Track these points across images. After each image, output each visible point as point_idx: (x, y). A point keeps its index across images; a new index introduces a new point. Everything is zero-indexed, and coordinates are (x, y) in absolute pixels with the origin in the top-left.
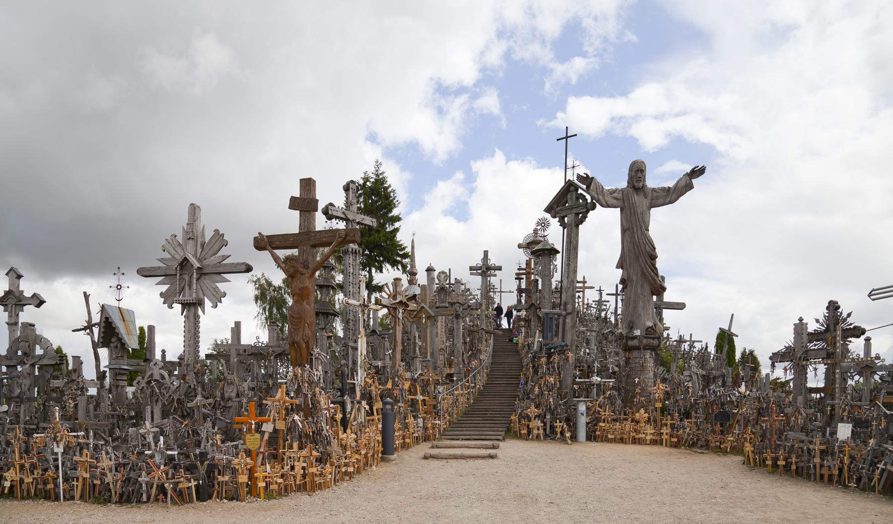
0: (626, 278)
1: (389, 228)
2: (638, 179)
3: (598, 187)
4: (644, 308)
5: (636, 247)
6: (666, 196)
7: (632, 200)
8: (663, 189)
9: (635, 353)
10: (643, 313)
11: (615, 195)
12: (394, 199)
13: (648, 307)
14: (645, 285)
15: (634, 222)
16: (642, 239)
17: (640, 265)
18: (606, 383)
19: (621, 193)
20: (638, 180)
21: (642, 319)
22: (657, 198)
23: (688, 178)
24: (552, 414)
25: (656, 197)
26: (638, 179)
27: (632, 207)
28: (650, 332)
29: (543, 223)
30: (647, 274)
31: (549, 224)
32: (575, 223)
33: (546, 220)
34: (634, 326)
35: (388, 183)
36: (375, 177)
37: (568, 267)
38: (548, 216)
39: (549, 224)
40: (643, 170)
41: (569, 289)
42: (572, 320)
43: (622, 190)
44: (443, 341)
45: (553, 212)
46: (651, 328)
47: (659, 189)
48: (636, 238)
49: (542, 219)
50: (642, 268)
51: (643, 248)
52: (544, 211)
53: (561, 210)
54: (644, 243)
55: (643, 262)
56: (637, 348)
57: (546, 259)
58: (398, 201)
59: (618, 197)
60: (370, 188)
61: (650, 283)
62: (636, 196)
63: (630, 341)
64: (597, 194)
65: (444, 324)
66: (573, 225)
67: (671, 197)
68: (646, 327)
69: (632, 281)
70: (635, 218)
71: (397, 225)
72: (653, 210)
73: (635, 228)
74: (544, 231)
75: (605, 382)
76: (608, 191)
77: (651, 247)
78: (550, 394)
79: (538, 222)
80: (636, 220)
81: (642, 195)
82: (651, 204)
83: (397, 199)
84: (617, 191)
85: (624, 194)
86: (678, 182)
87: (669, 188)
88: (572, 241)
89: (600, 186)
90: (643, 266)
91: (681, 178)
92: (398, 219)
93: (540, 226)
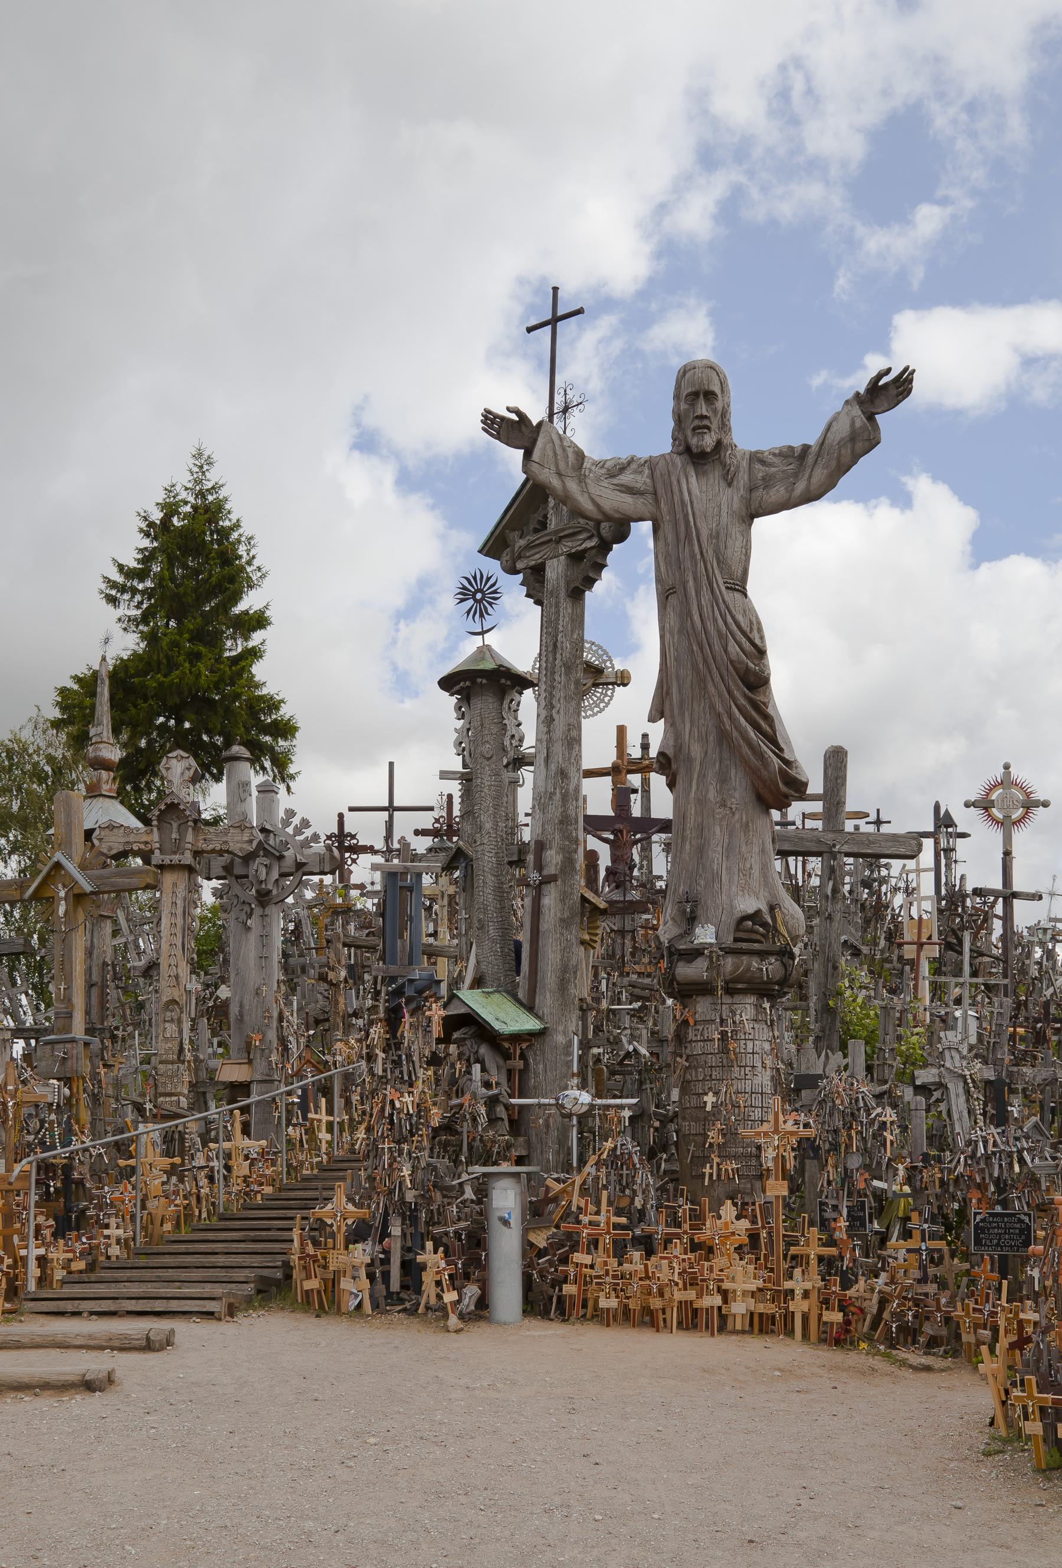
0: (670, 752)
1: (233, 647)
2: (697, 422)
3: (559, 451)
4: (729, 850)
6: (796, 475)
7: (681, 491)
8: (787, 454)
9: (702, 1007)
10: (729, 869)
11: (626, 478)
12: (249, 563)
13: (744, 849)
14: (733, 772)
15: (688, 564)
16: (715, 620)
17: (712, 707)
18: (611, 1113)
19: (647, 471)
20: (699, 427)
21: (725, 888)
22: (768, 482)
23: (857, 411)
24: (410, 1216)
25: (764, 479)
26: (697, 422)
27: (680, 516)
28: (752, 931)
30: (735, 734)
31: (495, 592)
33: (488, 579)
34: (700, 912)
35: (234, 517)
36: (191, 499)
37: (549, 727)
38: (492, 567)
39: (495, 592)
40: (713, 393)
41: (551, 798)
42: (563, 901)
43: (651, 464)
44: (177, 977)
45: (506, 556)
46: (755, 917)
47: (774, 455)
48: (696, 618)
50: (719, 715)
52: (480, 551)
54: (719, 631)
55: (720, 696)
56: (704, 989)
57: (484, 704)
58: (259, 569)
59: (638, 485)
60: (182, 531)
61: (745, 763)
62: (693, 479)
63: (680, 964)
64: (559, 474)
65: (179, 921)
66: (563, 594)
67: (810, 477)
68: (738, 915)
69: (690, 760)
70: (692, 551)
71: (257, 638)
72: (761, 525)
73: (691, 583)
74: (482, 616)
75: (607, 1107)
76: (603, 467)
77: (747, 645)
78: (401, 1152)
79: (464, 588)
80: (693, 556)
81: (715, 475)
82: (747, 502)
83: (256, 563)
84: (634, 466)
85: (657, 473)
86: (828, 429)
87: (806, 448)
88: (559, 645)
89: (570, 451)
90: (720, 708)
91: (839, 413)
92: (259, 621)
93: (471, 602)
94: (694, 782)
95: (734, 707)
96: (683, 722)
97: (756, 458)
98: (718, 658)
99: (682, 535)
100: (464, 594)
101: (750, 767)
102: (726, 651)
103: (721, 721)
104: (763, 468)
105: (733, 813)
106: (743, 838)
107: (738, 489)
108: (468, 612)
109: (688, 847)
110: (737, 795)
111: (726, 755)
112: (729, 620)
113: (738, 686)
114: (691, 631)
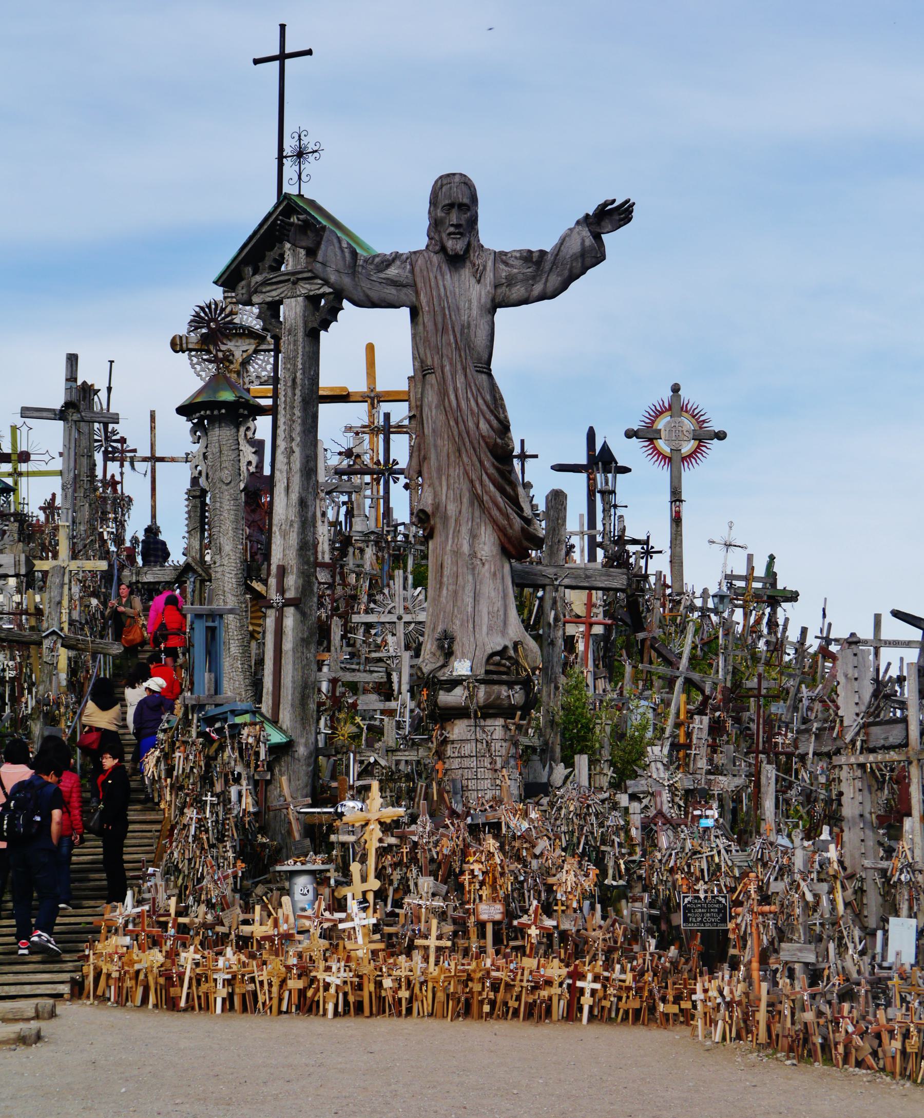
0: (429, 509)
5: (452, 423)
7: (438, 286)
14: (483, 528)
34: (456, 647)
46: (503, 652)
48: (452, 397)
50: (471, 481)
51: (471, 424)
61: (494, 522)
62: (448, 277)
63: (441, 692)
69: (445, 518)
73: (447, 368)
94: (451, 536)
96: (441, 484)
97: (501, 257)
98: (471, 433)
99: (440, 327)
101: (498, 526)
102: (478, 427)
103: (473, 486)
104: (507, 269)
105: (483, 564)
106: (492, 585)
107: (486, 286)
109: (445, 592)
110: (486, 548)
111: (477, 513)
114: (448, 409)
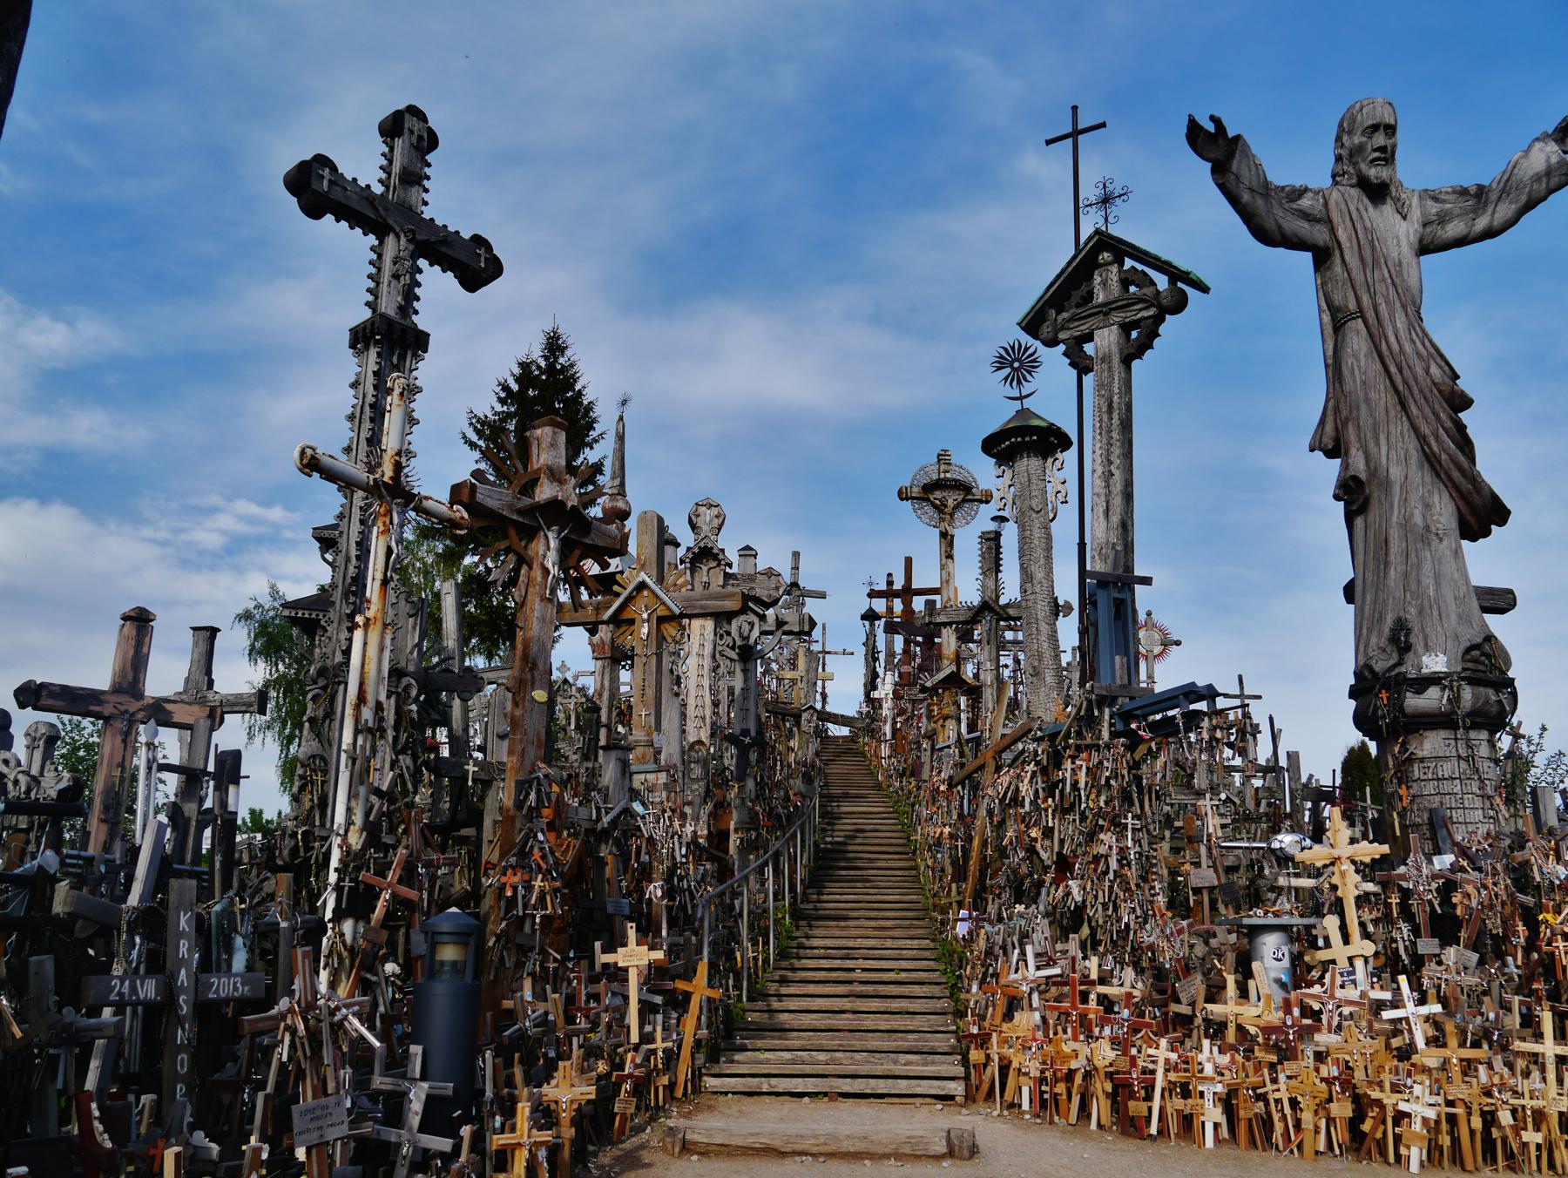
7: (1362, 218)
25: (1438, 214)
29: (1018, 360)
30: (1444, 457)
32: (1121, 350)
38: (1026, 339)
48: (1392, 339)
49: (1013, 348)
50: (1424, 437)
51: (1419, 370)
53: (1072, 319)
57: (1028, 464)
66: (1116, 361)
69: (1387, 484)
73: (1383, 308)
74: (1019, 383)
79: (1001, 357)
90: (1425, 429)
95: (1441, 430)
96: (1378, 445)
99: (1369, 260)
100: (1001, 363)
102: (1427, 372)
105: (1441, 540)
108: (1006, 379)
109: (1392, 573)
112: (1427, 344)
113: (1442, 407)
